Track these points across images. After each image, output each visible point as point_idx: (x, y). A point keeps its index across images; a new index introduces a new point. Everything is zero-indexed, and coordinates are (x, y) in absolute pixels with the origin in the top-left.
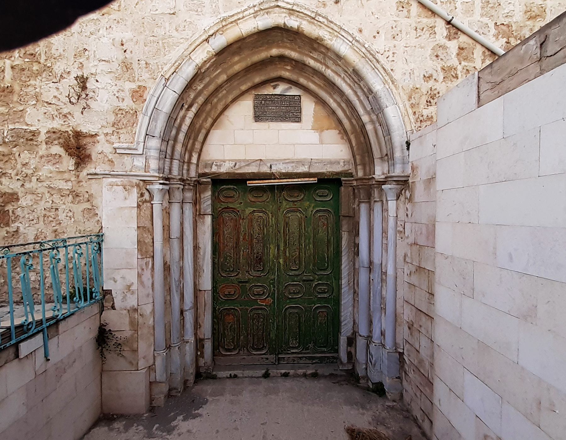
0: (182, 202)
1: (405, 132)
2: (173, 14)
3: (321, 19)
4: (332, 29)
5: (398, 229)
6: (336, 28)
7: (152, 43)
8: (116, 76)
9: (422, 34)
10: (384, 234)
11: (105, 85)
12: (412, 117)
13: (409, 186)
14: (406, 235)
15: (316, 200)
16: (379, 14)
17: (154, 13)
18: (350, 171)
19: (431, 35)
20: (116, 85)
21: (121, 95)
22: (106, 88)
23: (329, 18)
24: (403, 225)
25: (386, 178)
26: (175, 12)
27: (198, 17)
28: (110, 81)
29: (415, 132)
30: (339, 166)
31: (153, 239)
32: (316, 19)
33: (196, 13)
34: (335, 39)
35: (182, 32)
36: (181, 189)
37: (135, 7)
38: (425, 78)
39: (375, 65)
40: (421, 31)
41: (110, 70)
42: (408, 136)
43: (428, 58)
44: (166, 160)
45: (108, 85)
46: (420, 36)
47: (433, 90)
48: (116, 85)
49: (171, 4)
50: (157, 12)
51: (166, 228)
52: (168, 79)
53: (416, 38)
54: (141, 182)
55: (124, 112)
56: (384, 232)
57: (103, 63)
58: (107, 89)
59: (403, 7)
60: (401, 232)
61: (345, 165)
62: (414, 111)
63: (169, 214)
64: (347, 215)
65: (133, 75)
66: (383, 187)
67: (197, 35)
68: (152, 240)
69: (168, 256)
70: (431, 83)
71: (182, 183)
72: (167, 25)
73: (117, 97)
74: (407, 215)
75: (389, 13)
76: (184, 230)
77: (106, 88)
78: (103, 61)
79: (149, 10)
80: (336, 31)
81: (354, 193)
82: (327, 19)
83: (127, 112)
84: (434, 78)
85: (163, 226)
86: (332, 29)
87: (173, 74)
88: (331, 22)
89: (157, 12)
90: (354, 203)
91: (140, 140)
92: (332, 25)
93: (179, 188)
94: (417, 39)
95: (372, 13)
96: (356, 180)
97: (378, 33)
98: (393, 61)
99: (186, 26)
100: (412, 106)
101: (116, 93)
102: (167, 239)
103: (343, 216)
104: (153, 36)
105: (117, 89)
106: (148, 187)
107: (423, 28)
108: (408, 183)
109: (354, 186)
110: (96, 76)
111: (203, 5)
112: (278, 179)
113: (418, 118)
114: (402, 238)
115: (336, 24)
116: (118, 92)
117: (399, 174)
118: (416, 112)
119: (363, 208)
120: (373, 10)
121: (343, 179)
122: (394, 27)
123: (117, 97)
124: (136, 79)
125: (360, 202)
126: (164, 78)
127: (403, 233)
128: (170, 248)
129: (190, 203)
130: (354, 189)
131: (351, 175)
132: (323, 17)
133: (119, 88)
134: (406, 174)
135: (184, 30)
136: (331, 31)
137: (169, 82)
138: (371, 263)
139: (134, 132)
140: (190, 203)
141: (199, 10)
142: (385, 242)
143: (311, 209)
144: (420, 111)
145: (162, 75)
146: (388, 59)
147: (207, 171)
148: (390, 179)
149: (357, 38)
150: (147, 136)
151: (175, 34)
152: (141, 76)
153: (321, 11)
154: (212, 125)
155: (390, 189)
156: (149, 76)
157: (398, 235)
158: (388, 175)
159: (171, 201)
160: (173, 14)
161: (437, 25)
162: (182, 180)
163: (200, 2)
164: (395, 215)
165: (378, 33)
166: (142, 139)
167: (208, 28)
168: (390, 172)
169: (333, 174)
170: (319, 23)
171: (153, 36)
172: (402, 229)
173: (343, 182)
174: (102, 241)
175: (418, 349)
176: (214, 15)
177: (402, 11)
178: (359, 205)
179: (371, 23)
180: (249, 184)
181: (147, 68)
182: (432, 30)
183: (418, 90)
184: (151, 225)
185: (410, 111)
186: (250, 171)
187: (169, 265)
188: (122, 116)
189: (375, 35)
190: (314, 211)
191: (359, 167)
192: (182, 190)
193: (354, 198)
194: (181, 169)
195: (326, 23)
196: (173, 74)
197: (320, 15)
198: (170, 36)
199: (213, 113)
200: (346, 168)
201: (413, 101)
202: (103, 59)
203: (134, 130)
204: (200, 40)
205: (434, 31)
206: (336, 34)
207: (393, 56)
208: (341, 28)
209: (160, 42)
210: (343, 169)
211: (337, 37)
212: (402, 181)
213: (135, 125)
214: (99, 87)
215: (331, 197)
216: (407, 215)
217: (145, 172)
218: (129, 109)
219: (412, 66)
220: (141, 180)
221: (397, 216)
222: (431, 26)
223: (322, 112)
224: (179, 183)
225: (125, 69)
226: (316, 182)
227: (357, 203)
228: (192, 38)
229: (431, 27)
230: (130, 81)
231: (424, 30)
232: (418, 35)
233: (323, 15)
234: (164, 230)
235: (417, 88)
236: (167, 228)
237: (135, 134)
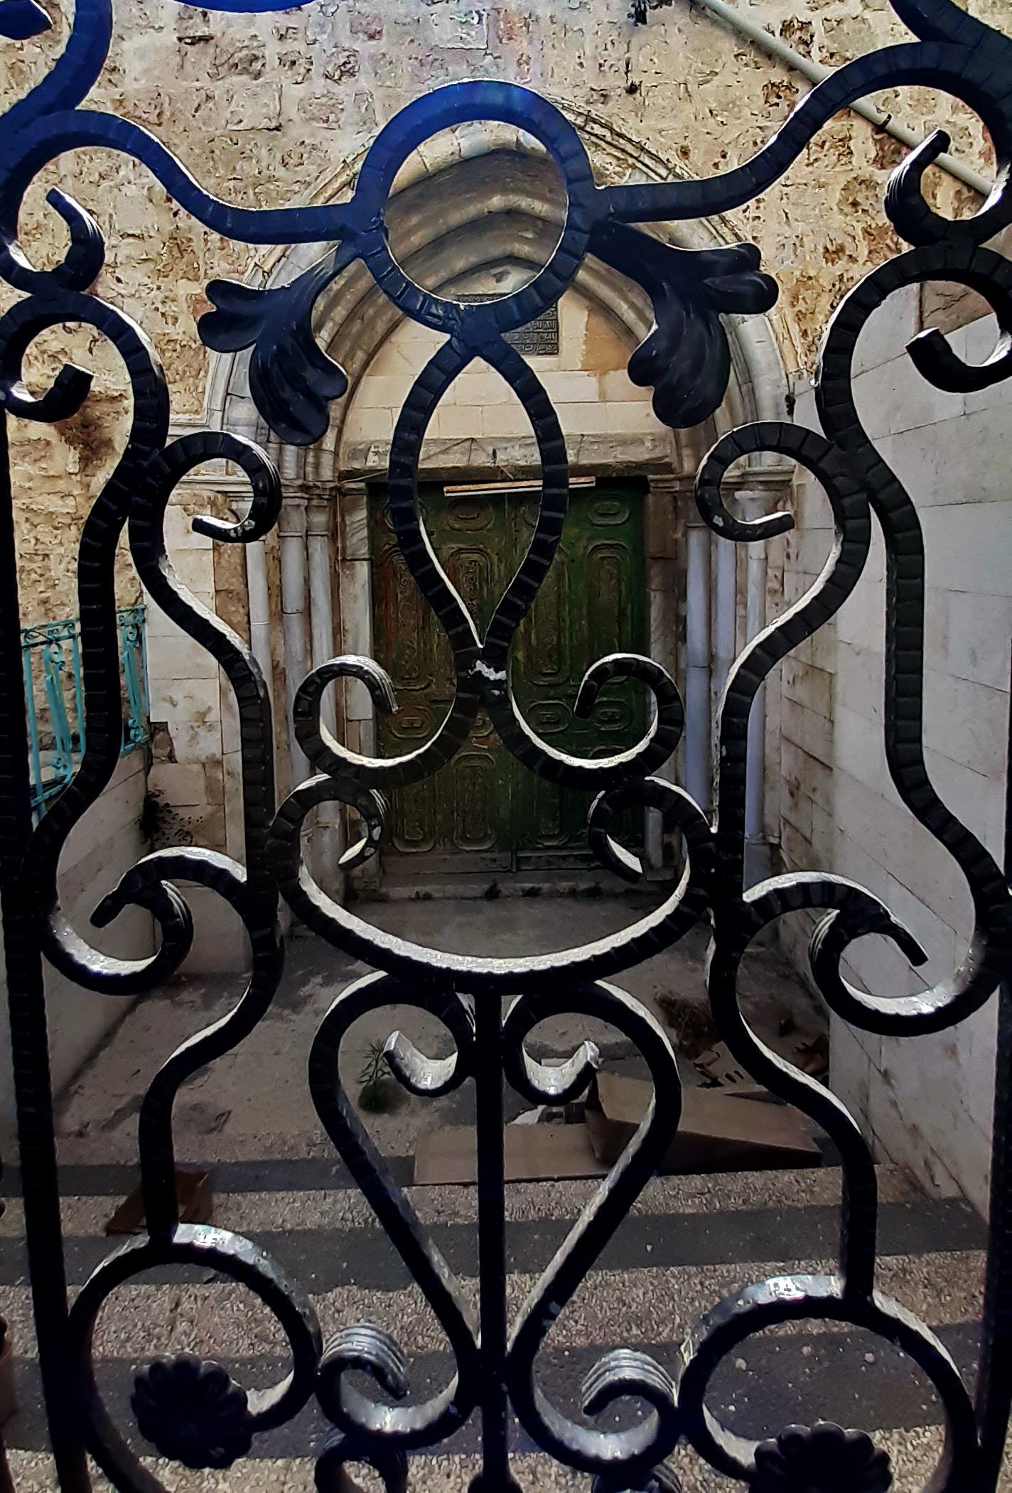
0: (307, 536)
1: (784, 376)
2: (277, 129)
3: (598, 130)
4: (623, 151)
5: (770, 585)
6: (630, 148)
7: (233, 195)
8: (158, 268)
9: (821, 155)
10: (739, 596)
11: (137, 287)
12: (798, 341)
13: (792, 493)
14: (786, 597)
15: (593, 525)
16: (725, 113)
17: (235, 128)
18: (667, 460)
19: (841, 157)
20: (159, 288)
21: (170, 308)
22: (137, 295)
23: (615, 127)
24: (780, 577)
25: (743, 475)
26: (280, 125)
27: (329, 134)
28: (146, 281)
29: (805, 374)
30: (643, 449)
31: (248, 615)
32: (588, 129)
33: (325, 125)
34: (628, 172)
35: (296, 169)
36: (303, 508)
37: (194, 116)
38: (827, 255)
39: (718, 228)
40: (819, 149)
41: (144, 257)
42: (791, 383)
43: (835, 208)
44: (271, 445)
45: (142, 288)
46: (816, 160)
47: (845, 280)
48: (159, 288)
49: (272, 107)
50: (240, 127)
51: (275, 591)
52: (270, 273)
53: (808, 165)
54: (219, 496)
55: (178, 347)
56: (740, 591)
57: (131, 240)
58: (140, 297)
59: (779, 97)
60: (776, 591)
61: (655, 447)
62: (803, 328)
63: (280, 561)
64: (661, 555)
65: (196, 265)
66: (738, 494)
67: (328, 175)
68: (246, 618)
69: (281, 650)
70: (841, 265)
71: (306, 496)
72: (264, 152)
73: (163, 314)
74: (788, 556)
75: (747, 112)
76: (312, 595)
77: (137, 295)
78: (129, 235)
79: (224, 123)
80: (631, 156)
81: (675, 508)
82: (611, 130)
83: (185, 346)
84: (847, 253)
85: (269, 589)
86: (623, 151)
87: (279, 261)
88: (621, 136)
89: (240, 127)
90: (675, 530)
91: (214, 407)
92: (621, 141)
93: (298, 506)
94: (810, 168)
95: (711, 112)
96: (679, 479)
97: (724, 156)
98: (759, 218)
99: (305, 156)
100: (800, 317)
101: (160, 306)
102: (278, 614)
103: (656, 559)
104: (235, 179)
105: (161, 296)
106: (234, 505)
107: (824, 142)
108: (790, 487)
109: (676, 492)
110: (117, 270)
111: (340, 107)
112: (510, 480)
113: (813, 342)
114: (777, 605)
115: (630, 140)
116: (163, 302)
117: (771, 468)
118: (809, 332)
119: (696, 540)
120: (713, 106)
121: (651, 477)
122: (758, 141)
123: (163, 314)
124: (202, 273)
125: (687, 529)
126: (261, 270)
127: (779, 595)
128: (284, 633)
129: (322, 536)
130: (675, 498)
131: (668, 468)
132: (602, 126)
133: (167, 294)
134: (785, 468)
135: (302, 164)
136: (619, 154)
137: (272, 277)
138: (712, 657)
139: (200, 390)
140: (322, 536)
141: (332, 117)
142: (741, 612)
143: (583, 542)
144: (818, 327)
145: (256, 265)
146: (747, 214)
147: (357, 465)
148: (751, 479)
149: (678, 170)
150: (229, 398)
151: (280, 172)
152: (212, 268)
153: (598, 110)
154: (366, 365)
155: (753, 499)
156: (228, 267)
157: (769, 598)
158: (748, 469)
159: (282, 534)
160: (277, 129)
161: (853, 134)
162: (304, 488)
163: (334, 101)
164: (763, 556)
165: (724, 156)
166: (217, 405)
167: (352, 157)
168: (753, 463)
169: (629, 466)
170: (593, 139)
171: (235, 179)
172: (776, 585)
173: (652, 484)
174: (144, 621)
175: (808, 834)
176: (365, 127)
177: (777, 104)
178: (685, 535)
179: (708, 133)
180: (448, 492)
181: (223, 249)
182: (843, 146)
183: (814, 281)
184: (242, 586)
185: (795, 330)
186: (450, 465)
187: (284, 669)
188: (175, 355)
189: (716, 160)
190: (591, 548)
191: (686, 452)
192: (306, 508)
193: (677, 518)
194: (301, 464)
195: (609, 138)
196: (279, 261)
197: (595, 121)
198: (272, 179)
199: (366, 338)
200: (657, 453)
201: (801, 306)
202: (130, 232)
203: (201, 384)
204: (336, 185)
205: (849, 148)
206: (631, 161)
207: (758, 208)
208: (642, 149)
209: (251, 192)
210: (653, 456)
211: (633, 167)
212: (777, 482)
213: (202, 373)
214: (123, 292)
215: (627, 516)
216: (788, 556)
217: (228, 474)
218: (188, 338)
219: (800, 227)
220: (218, 492)
221: (766, 558)
222: (840, 137)
223: (603, 329)
224: (299, 494)
225: (176, 253)
226: (594, 485)
227: (681, 529)
228: (319, 180)
229: (840, 140)
230: (189, 279)
231: (826, 147)
232: (811, 160)
233: (603, 121)
234: (270, 595)
235: (810, 278)
236: (276, 591)
237: (203, 392)
